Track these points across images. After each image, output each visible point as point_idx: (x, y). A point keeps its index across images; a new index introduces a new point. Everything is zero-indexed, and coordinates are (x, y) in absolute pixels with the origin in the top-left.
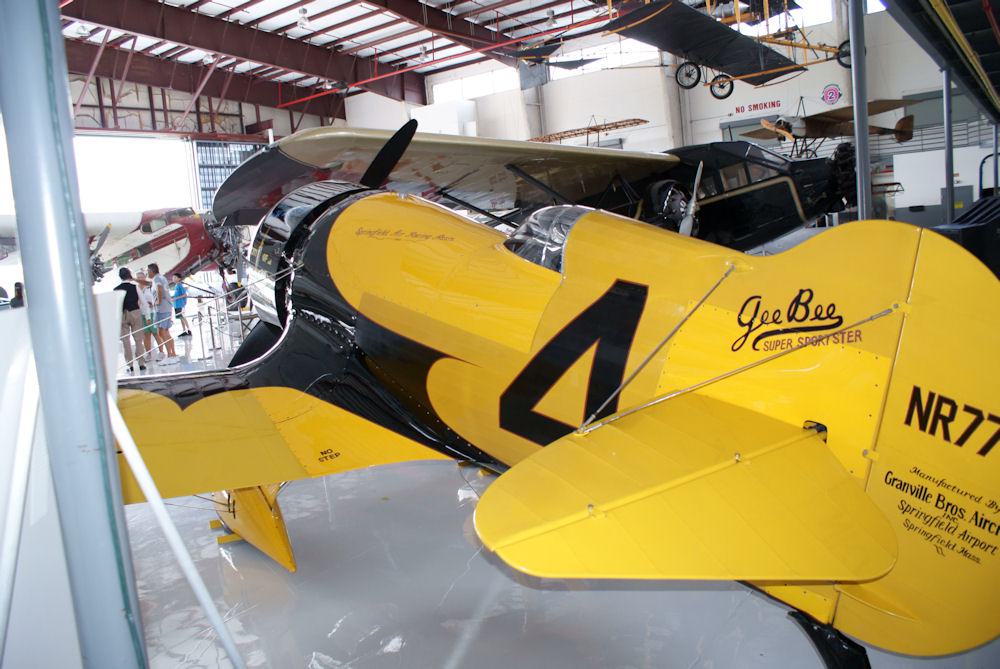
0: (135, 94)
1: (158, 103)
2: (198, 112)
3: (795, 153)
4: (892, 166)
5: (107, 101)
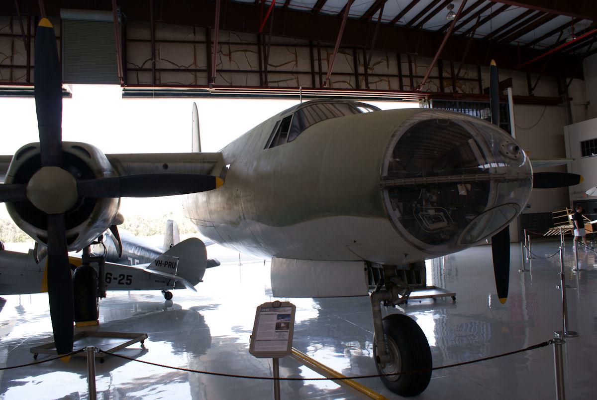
0: (385, 62)
1: (405, 70)
2: (441, 78)
5: (361, 70)
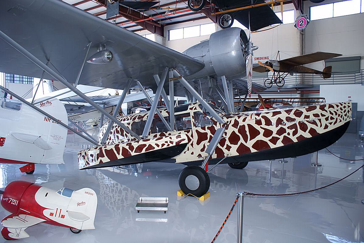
3: (274, 78)
4: (319, 91)
